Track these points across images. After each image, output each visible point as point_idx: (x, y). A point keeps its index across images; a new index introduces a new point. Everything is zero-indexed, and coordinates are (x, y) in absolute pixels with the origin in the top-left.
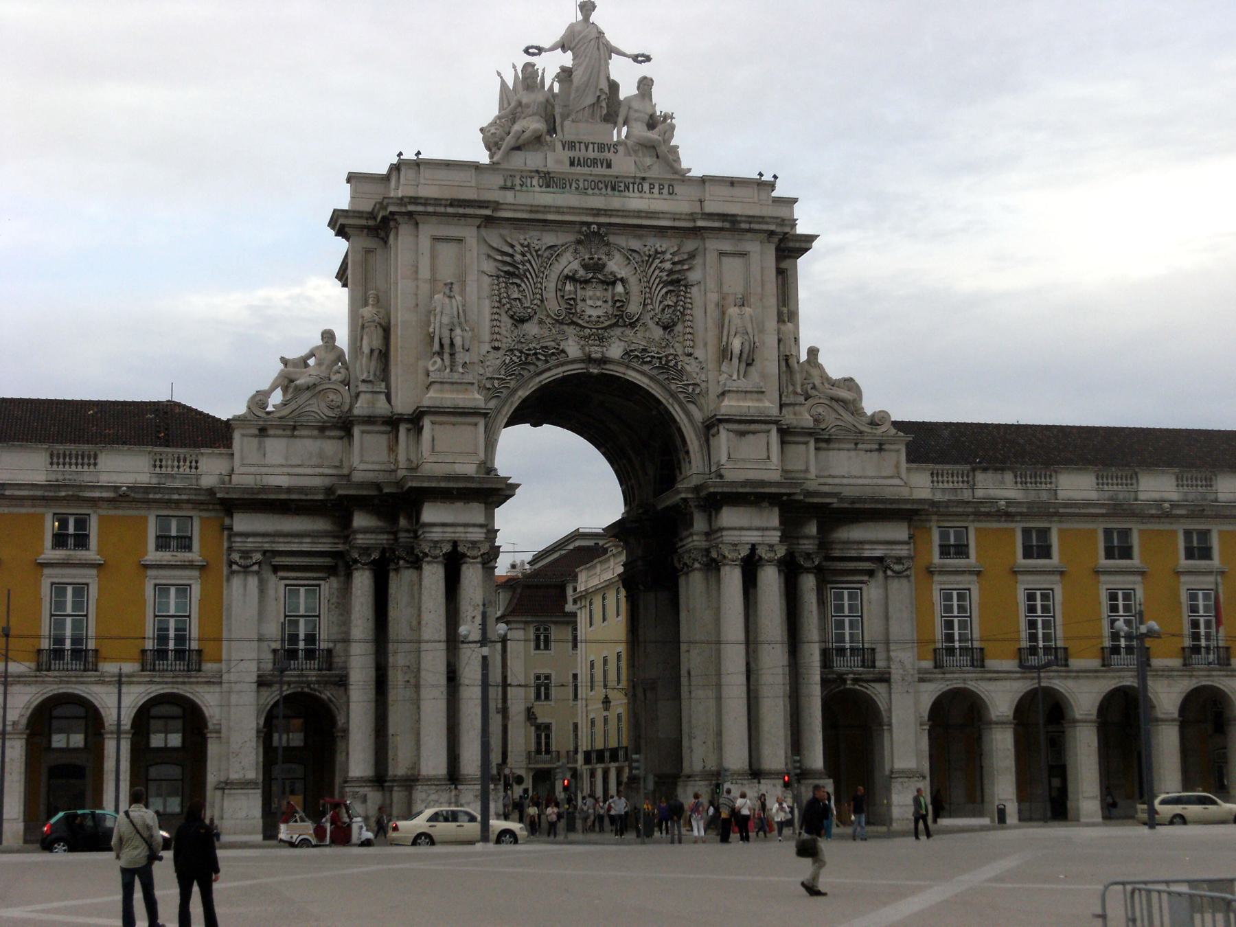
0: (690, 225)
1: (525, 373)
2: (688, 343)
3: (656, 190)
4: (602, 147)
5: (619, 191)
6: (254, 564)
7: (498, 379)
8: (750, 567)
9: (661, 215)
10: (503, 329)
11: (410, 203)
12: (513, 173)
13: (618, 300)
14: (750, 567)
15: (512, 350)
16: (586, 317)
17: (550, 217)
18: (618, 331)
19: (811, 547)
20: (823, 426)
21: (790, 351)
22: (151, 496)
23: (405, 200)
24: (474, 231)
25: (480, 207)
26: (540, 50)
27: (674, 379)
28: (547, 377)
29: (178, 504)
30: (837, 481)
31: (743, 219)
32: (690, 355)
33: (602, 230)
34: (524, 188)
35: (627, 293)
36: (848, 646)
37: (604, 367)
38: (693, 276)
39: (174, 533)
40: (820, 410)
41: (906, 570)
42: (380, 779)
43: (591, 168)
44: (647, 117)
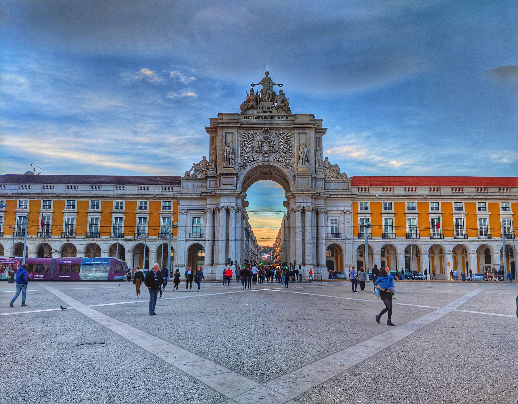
0: (291, 126)
1: (249, 165)
2: (290, 156)
3: (283, 118)
4: (269, 108)
8: (303, 211)
14: (303, 211)
17: (255, 126)
20: (328, 177)
24: (237, 130)
26: (255, 85)
28: (254, 166)
29: (167, 198)
30: (332, 191)
32: (291, 159)
33: (268, 129)
34: (249, 119)
36: (334, 232)
39: (167, 206)
42: (212, 265)
44: (282, 100)
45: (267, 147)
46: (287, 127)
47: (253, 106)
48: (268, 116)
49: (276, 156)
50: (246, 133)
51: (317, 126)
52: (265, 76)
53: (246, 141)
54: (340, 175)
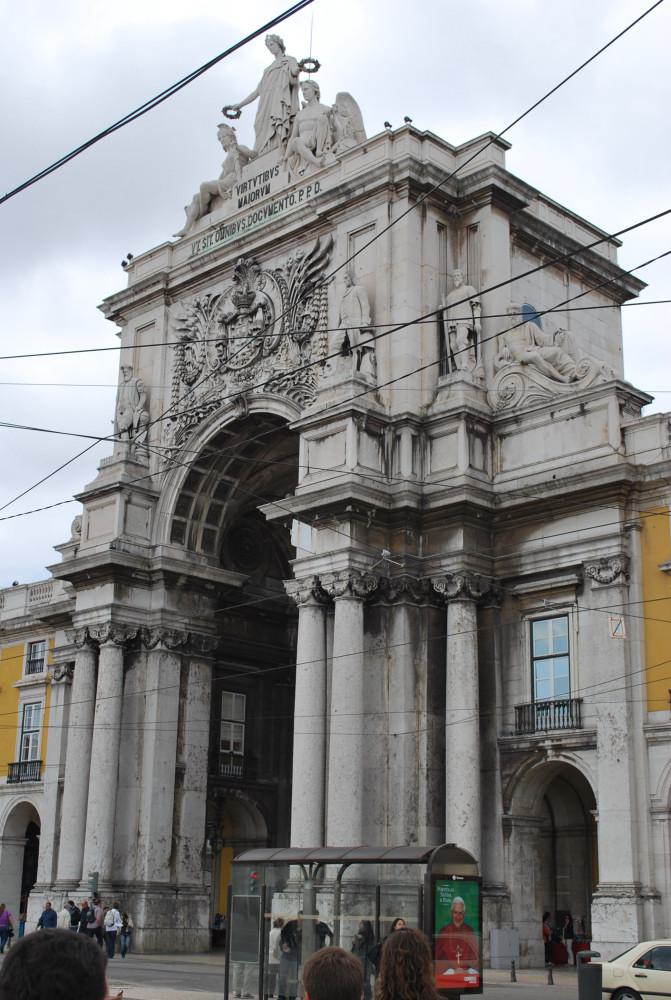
0: (314, 218)
4: (266, 176)
6: (63, 676)
7: (171, 450)
8: (325, 603)
9: (288, 220)
11: (112, 304)
12: (197, 240)
14: (325, 603)
18: (263, 364)
19: (455, 567)
22: (16, 627)
25: (154, 284)
30: (529, 471)
31: (354, 184)
35: (269, 318)
37: (250, 407)
40: (508, 383)
41: (617, 575)
48: (256, 210)
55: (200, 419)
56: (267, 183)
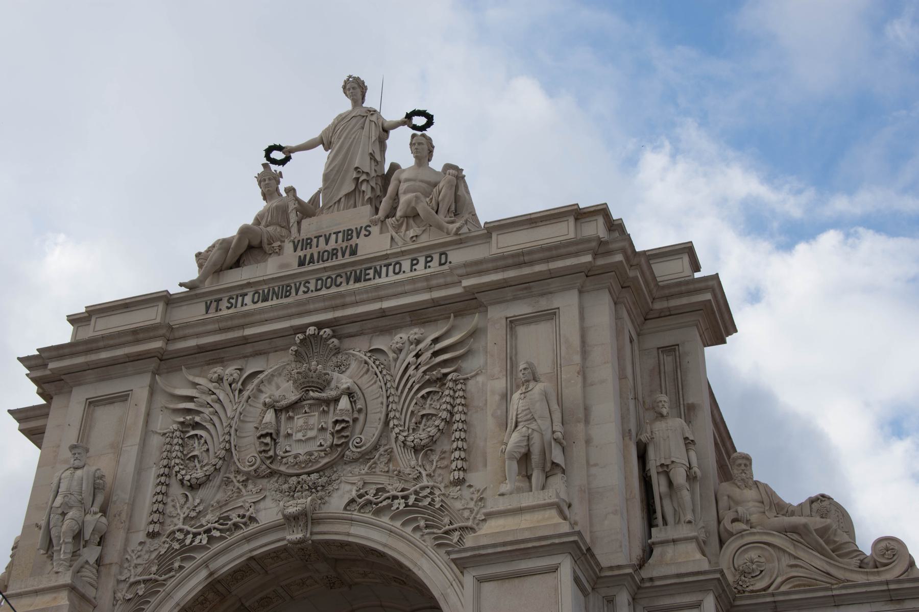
0: (457, 290)
1: (189, 565)
4: (348, 234)
5: (365, 280)
7: (145, 581)
10: (170, 504)
11: (52, 359)
13: (336, 422)
15: (173, 532)
16: (291, 460)
17: (249, 332)
21: (670, 458)
23: (45, 355)
24: (146, 379)
26: (288, 153)
27: (427, 527)
28: (225, 563)
32: (459, 482)
34: (230, 311)
38: (470, 365)
43: (330, 261)
45: (311, 434)
46: (435, 303)
47: (260, 247)
49: (368, 479)
50: (198, 380)
51: (619, 257)
52: (345, 105)
53: (197, 425)
54: (856, 561)
55: (211, 539)
56: (353, 242)
